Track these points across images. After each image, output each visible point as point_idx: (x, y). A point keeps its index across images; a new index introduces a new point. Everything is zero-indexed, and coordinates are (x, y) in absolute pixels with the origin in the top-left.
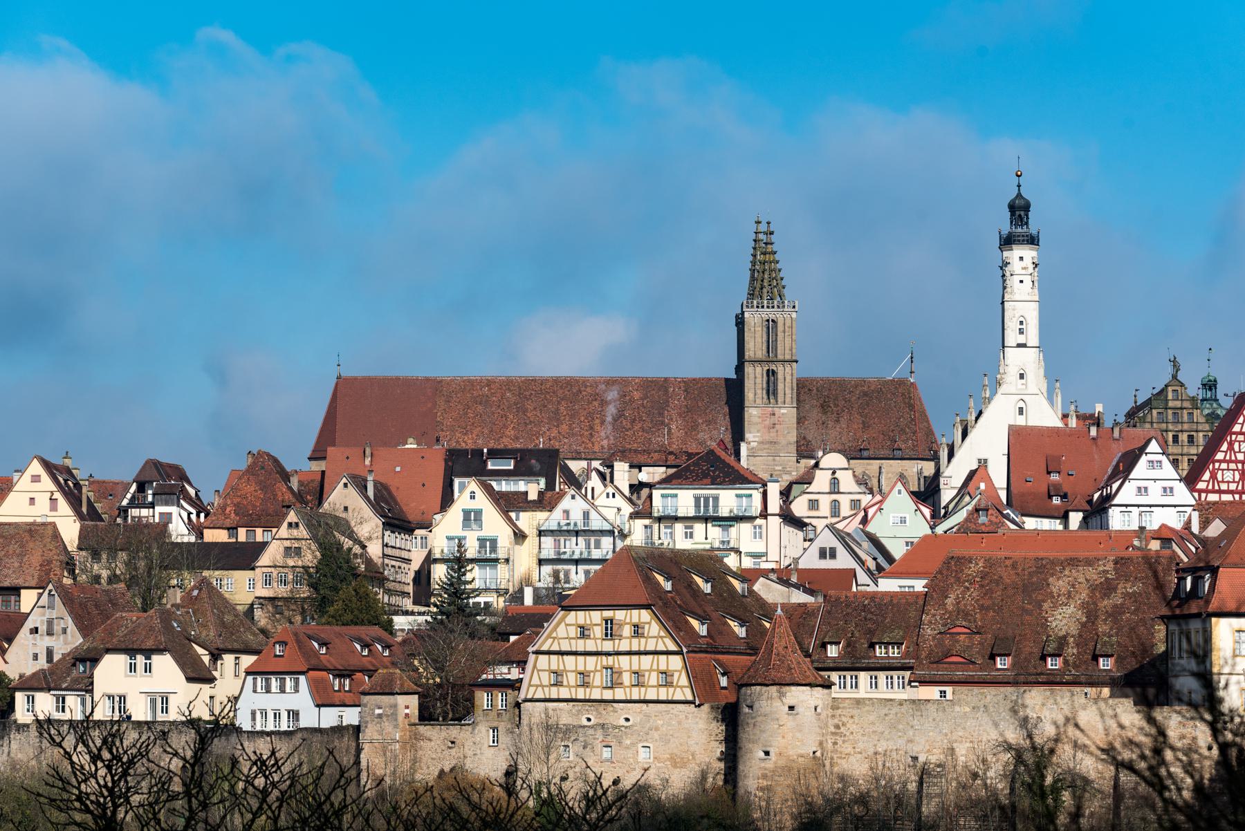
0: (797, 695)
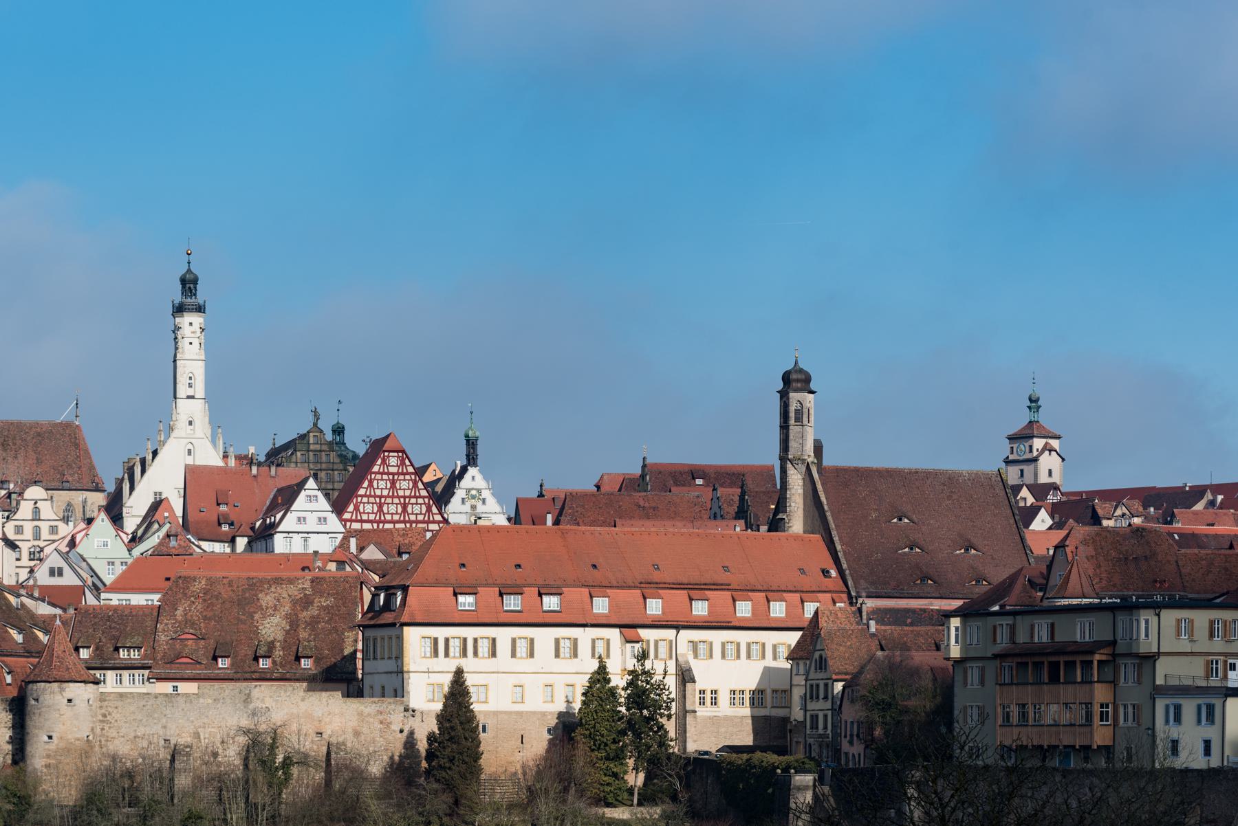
0: (74, 690)
